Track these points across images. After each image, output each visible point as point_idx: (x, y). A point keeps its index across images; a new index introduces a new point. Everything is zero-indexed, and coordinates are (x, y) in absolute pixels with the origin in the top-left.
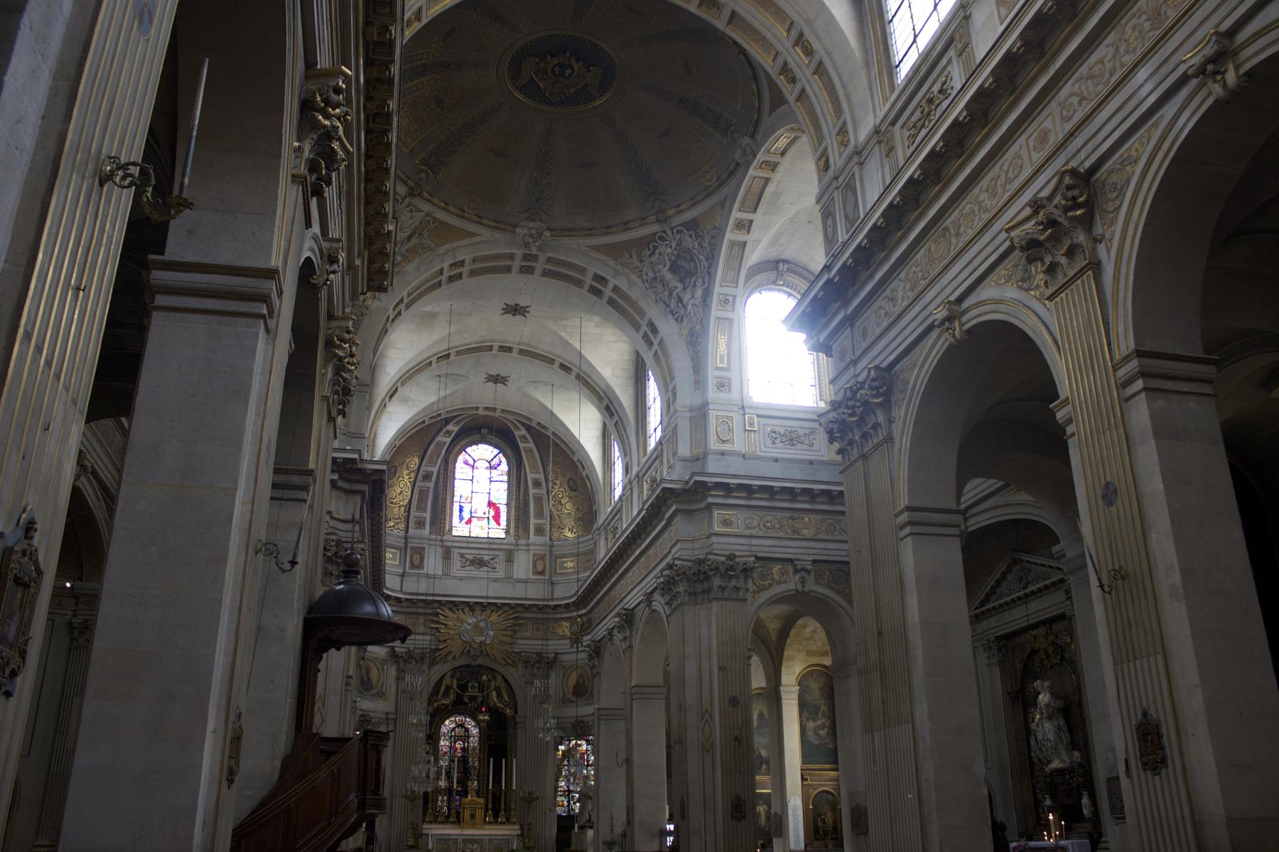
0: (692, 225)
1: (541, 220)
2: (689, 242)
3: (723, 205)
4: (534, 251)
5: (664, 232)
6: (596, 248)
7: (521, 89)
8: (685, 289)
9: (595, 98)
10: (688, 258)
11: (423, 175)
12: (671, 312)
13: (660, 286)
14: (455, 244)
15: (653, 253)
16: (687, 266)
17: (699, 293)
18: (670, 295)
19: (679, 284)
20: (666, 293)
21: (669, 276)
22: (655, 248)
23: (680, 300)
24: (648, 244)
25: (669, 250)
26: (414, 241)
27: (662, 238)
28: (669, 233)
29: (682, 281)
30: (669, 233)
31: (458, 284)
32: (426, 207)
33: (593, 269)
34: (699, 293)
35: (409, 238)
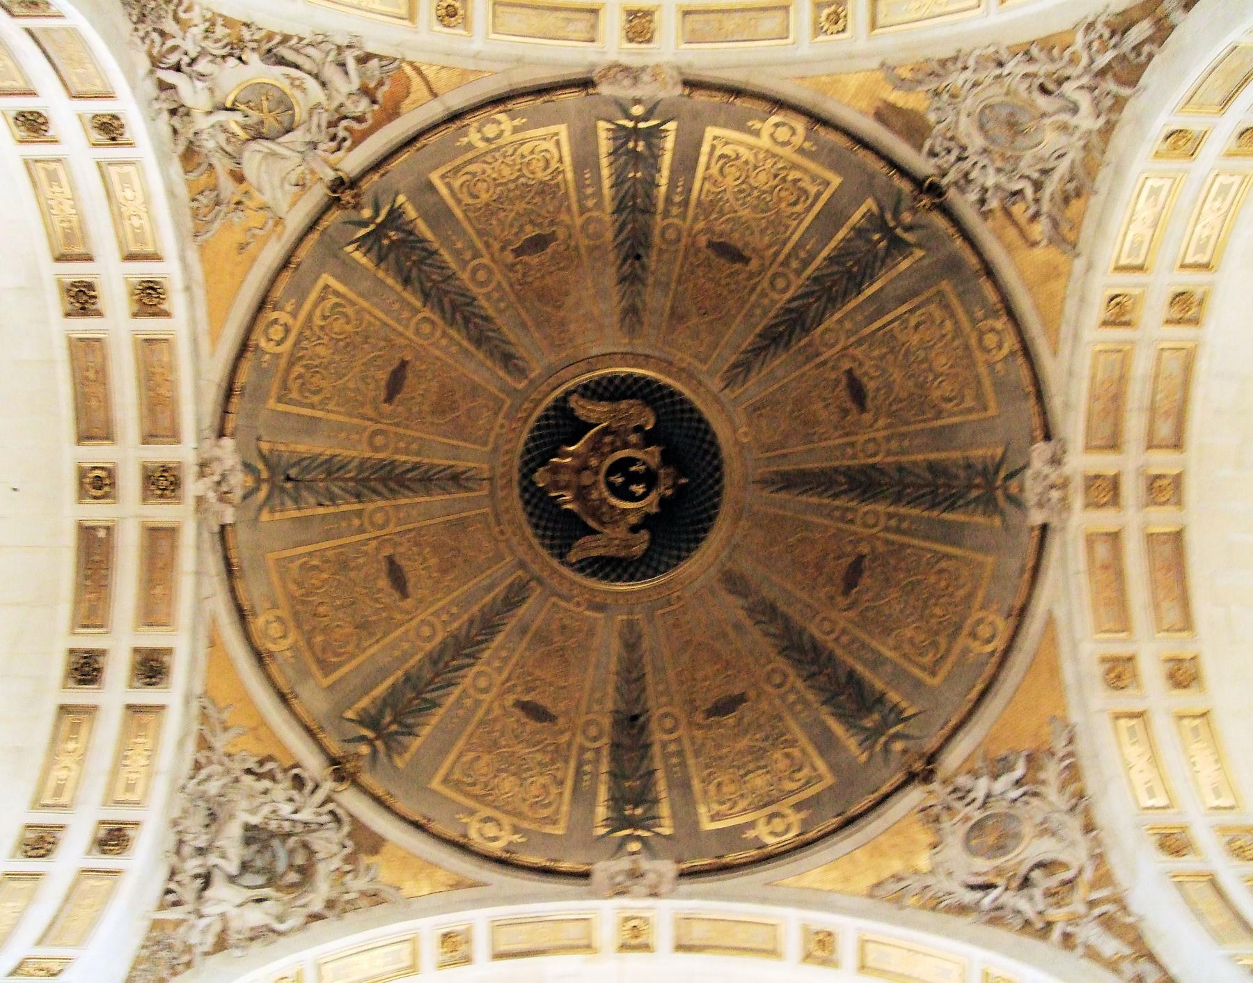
0: (366, 843)
1: (245, 497)
2: (329, 845)
3: (458, 885)
4: (193, 487)
5: (317, 787)
6: (214, 642)
7: (561, 408)
8: (232, 879)
9: (561, 556)
10: (300, 860)
11: (367, 213)
12: (173, 873)
13: (200, 817)
14: (199, 293)
15: (260, 776)
16: (281, 865)
17: (256, 916)
18: (201, 851)
19: (233, 868)
20: (202, 842)
21: (234, 831)
22: (271, 776)
23: (206, 880)
24: (270, 758)
25: (286, 809)
26: (228, 188)
27: (298, 782)
28: (320, 795)
29: (245, 867)
30: (320, 795)
31: (54, 303)
32: (296, 219)
33: (180, 642)
34: (256, 916)
35: (239, 178)
